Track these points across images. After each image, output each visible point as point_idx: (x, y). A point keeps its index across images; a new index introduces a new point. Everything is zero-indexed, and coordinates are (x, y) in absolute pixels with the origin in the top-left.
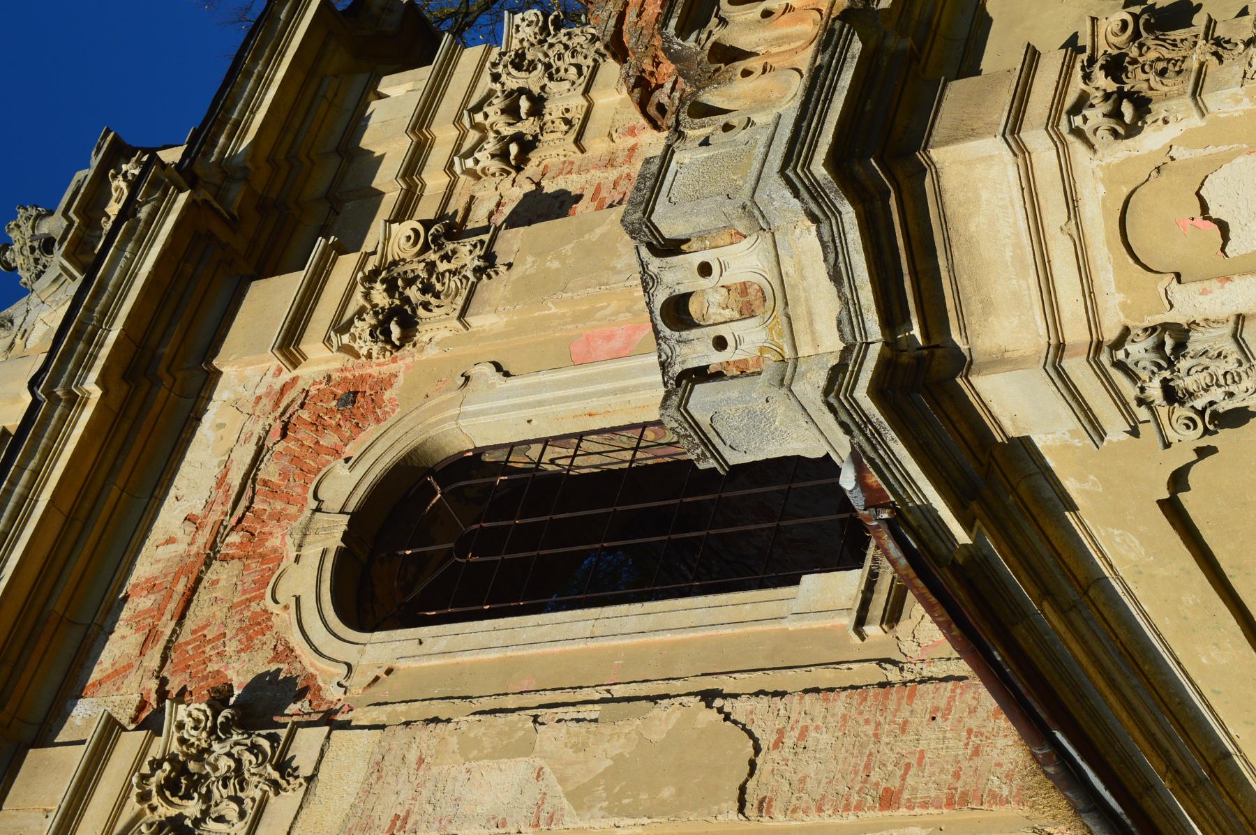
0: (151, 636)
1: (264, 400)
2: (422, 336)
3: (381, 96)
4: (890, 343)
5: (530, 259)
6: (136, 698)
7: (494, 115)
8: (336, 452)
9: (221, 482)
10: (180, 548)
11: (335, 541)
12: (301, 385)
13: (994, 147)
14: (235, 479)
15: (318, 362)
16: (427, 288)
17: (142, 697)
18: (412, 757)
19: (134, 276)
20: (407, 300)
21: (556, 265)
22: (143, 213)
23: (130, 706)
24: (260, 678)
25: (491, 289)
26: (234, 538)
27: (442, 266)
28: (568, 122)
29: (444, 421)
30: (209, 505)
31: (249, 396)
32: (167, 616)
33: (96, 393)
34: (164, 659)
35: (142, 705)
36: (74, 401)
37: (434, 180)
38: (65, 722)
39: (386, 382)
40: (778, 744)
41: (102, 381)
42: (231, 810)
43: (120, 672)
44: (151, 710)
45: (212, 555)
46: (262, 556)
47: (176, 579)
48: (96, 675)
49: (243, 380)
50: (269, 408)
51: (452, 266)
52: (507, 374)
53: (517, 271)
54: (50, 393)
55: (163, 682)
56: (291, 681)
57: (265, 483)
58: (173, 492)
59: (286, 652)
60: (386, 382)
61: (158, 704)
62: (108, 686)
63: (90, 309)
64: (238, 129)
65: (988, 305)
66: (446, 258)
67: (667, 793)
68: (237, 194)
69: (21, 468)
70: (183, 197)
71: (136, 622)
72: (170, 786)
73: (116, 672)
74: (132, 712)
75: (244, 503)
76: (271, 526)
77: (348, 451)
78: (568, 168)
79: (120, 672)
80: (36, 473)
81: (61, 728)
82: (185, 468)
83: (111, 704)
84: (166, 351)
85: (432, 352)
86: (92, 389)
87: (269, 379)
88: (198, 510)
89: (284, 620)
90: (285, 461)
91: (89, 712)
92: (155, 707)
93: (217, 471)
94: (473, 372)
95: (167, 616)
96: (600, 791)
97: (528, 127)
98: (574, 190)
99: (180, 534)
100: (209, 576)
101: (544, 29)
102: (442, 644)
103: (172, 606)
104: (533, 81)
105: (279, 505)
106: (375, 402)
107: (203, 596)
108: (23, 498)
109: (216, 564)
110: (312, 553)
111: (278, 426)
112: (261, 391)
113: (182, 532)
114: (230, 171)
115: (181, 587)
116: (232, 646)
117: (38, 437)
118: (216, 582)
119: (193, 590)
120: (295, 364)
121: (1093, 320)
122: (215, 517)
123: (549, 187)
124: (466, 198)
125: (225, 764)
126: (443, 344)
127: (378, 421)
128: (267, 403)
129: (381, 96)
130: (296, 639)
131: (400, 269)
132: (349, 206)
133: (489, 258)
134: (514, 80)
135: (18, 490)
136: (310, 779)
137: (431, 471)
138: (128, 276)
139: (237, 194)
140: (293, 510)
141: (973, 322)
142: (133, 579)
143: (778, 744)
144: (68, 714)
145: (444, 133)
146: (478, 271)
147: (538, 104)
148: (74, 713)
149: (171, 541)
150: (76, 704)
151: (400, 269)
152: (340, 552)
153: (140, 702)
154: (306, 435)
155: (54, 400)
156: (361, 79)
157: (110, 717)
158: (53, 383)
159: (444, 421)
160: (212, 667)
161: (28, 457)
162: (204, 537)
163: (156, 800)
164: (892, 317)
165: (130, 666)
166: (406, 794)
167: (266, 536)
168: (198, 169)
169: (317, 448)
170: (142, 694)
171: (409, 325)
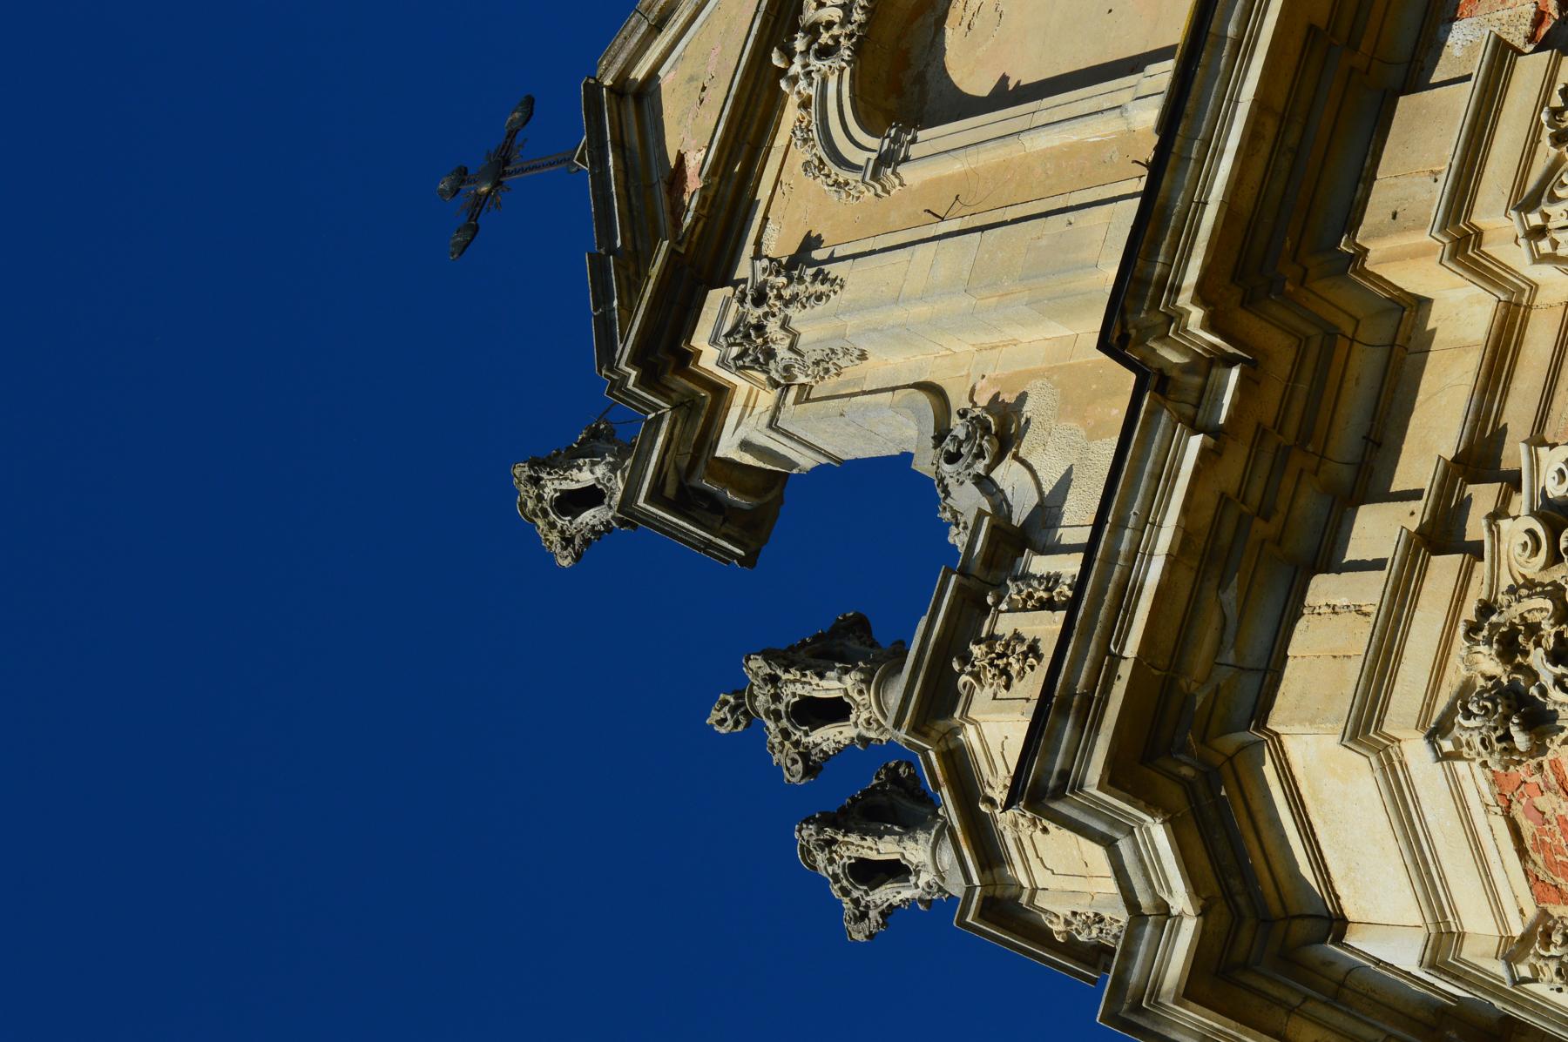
17: (1537, 7)
23: (1524, 21)
38: (1441, 55)
44: (1552, 22)
61: (1560, 13)
74: (1526, 28)
81: (1436, 63)
83: (1497, 23)
91: (1470, 38)
92: (1557, 17)
144: (1441, 44)
148: (1450, 41)
150: (1450, 30)
153: (1536, 14)
157: (1498, 39)
170: (1536, 3)
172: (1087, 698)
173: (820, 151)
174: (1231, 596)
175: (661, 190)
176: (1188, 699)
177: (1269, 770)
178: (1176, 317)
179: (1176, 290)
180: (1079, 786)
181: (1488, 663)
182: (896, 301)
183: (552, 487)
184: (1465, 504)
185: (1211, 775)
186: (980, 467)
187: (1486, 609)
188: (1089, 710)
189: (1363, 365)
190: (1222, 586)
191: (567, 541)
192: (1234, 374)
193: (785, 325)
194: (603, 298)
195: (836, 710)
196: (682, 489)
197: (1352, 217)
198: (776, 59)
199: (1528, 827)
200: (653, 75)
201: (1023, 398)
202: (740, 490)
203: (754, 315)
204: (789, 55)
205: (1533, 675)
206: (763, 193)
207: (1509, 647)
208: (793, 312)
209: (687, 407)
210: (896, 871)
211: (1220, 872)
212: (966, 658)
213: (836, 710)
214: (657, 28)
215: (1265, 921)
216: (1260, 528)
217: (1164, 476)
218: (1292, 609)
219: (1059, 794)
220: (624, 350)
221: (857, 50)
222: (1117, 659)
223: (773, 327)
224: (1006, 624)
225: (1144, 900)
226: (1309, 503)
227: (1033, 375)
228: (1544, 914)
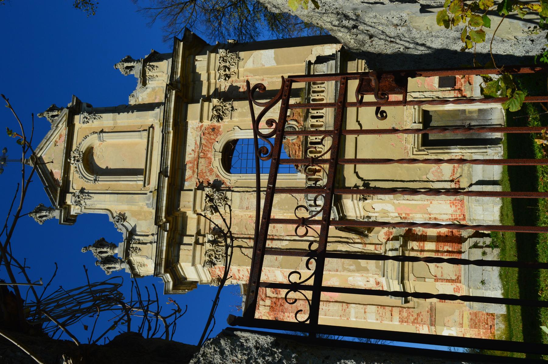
0: (194, 172)
1: (198, 128)
2: (224, 120)
3: (197, 60)
4: (339, 217)
5: (240, 109)
6: (195, 183)
7: (222, 72)
8: (214, 140)
9: (196, 143)
10: (193, 155)
11: (221, 157)
12: (204, 126)
13: (351, 200)
14: (198, 143)
15: (206, 122)
16: (223, 112)
18: (246, 197)
19: (171, 108)
20: (219, 113)
21: (245, 111)
22: (168, 96)
24: (215, 180)
25: (235, 113)
26: (202, 154)
27: (224, 108)
28: (235, 73)
29: (232, 136)
30: (195, 148)
31: (195, 127)
32: (195, 168)
33: (172, 131)
34: (197, 176)
35: (197, 184)
36: (168, 133)
37: (212, 81)
39: (219, 127)
40: (300, 200)
41: (172, 130)
42: (220, 205)
43: (191, 177)
45: (199, 157)
46: (208, 158)
47: (194, 162)
48: (186, 178)
49: (193, 123)
50: (200, 130)
51: (226, 108)
52: (241, 129)
53: (238, 111)
54: (165, 133)
55: (199, 180)
56: (220, 181)
57: (204, 144)
58: (187, 145)
59: (217, 176)
60: (219, 127)
62: (189, 180)
63: (166, 116)
64: (176, 73)
65: (348, 212)
66: (225, 106)
67: (287, 207)
68: (180, 86)
69: (165, 146)
70: (174, 92)
71: (190, 168)
72: (209, 201)
73: (190, 177)
75: (201, 148)
76: (207, 153)
77: (217, 140)
78: (236, 81)
79: (191, 177)
80: (167, 146)
82: (188, 140)
84: (179, 120)
85: (226, 123)
86: (171, 129)
87: (197, 124)
88: (194, 149)
89: (215, 170)
90: (206, 140)
93: (194, 142)
94: (234, 127)
95: (195, 168)
96: (277, 206)
97: (227, 72)
98: (239, 86)
99: (192, 153)
100: (200, 161)
101: (226, 53)
102: (244, 178)
103: (195, 166)
104: (227, 64)
105: (208, 149)
106: (218, 131)
107: (200, 164)
108: (167, 151)
109: (200, 159)
110: (217, 159)
111: (202, 133)
112: (197, 126)
113: (192, 153)
114: (177, 81)
115: (196, 163)
116: (208, 174)
117: (165, 140)
118: (201, 162)
119: (198, 163)
120: (202, 123)
121: (360, 214)
122: (197, 150)
123: (234, 84)
124: (219, 85)
125: (217, 197)
126: (228, 122)
127: (220, 135)
128: (199, 129)
129: (197, 60)
130: (219, 174)
131: (217, 108)
132: (197, 82)
133: (232, 107)
134: (223, 64)
135: (166, 150)
136: (231, 200)
137: (230, 142)
138: (170, 108)
139: (180, 86)
140: (210, 150)
141: (347, 213)
142: (186, 160)
143: (300, 200)
145: (212, 72)
146: (232, 110)
147: (229, 69)
149: (191, 154)
151: (217, 108)
152: (221, 159)
154: (207, 135)
155: (166, 133)
156: (192, 56)
158: (165, 131)
159: (232, 136)
160: (206, 177)
161: (165, 144)
162: (196, 154)
163: (208, 202)
164: (339, 214)
165: (192, 177)
166: (247, 203)
167: (207, 154)
168: (172, 83)
169: (211, 139)
171: (222, 119)
172: (160, 263)
173: (81, 175)
174: (172, 249)
175: (49, 175)
176: (170, 261)
177: (179, 266)
178: (162, 220)
179: (162, 217)
180: (161, 273)
181: (207, 258)
182: (105, 202)
183: (38, 215)
184: (199, 238)
185: (173, 268)
186: (122, 223)
187: (206, 252)
188: (160, 265)
189: (180, 219)
190: (171, 248)
191: (41, 221)
192: (168, 224)
193: (84, 202)
194: (50, 195)
195: (106, 252)
196: (66, 219)
197: (179, 206)
198: (69, 161)
199: (210, 271)
200: (41, 156)
201: (125, 213)
202: (74, 217)
203: (78, 200)
204: (70, 160)
205: (212, 259)
206: (71, 179)
207: (209, 256)
208: (86, 200)
209: (65, 209)
210: (115, 268)
211: (174, 277)
212: (130, 250)
213: (106, 252)
214: (41, 150)
215: (178, 280)
216: (174, 240)
217: (163, 237)
218: (179, 249)
219: (159, 274)
220: (57, 204)
221: (83, 160)
222: (162, 258)
223: (82, 202)
224: (134, 246)
225: (166, 281)
226: (178, 236)
227: (126, 210)
228: (212, 279)
